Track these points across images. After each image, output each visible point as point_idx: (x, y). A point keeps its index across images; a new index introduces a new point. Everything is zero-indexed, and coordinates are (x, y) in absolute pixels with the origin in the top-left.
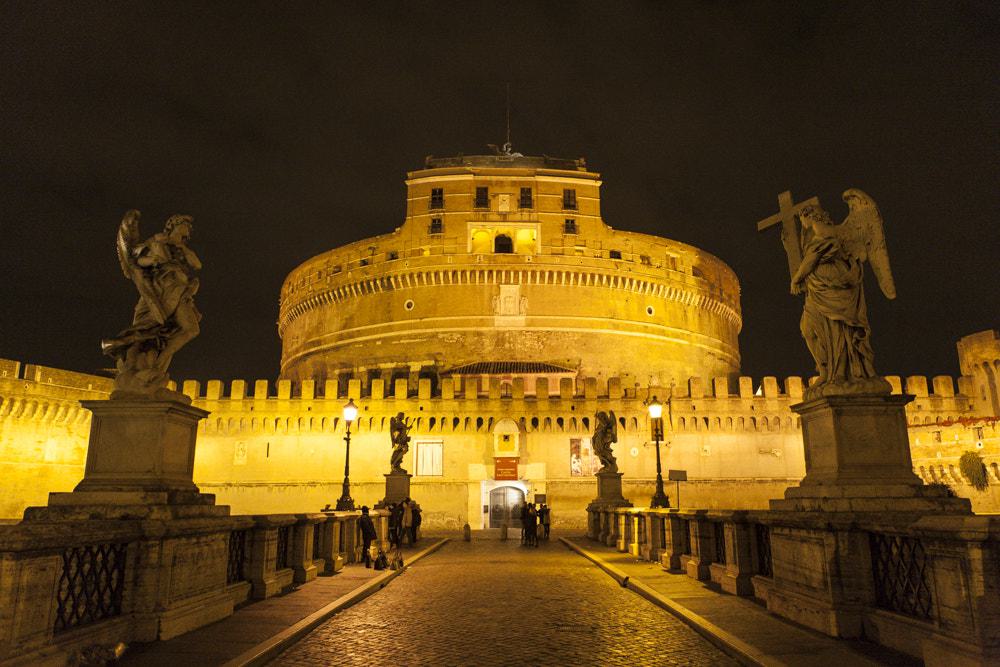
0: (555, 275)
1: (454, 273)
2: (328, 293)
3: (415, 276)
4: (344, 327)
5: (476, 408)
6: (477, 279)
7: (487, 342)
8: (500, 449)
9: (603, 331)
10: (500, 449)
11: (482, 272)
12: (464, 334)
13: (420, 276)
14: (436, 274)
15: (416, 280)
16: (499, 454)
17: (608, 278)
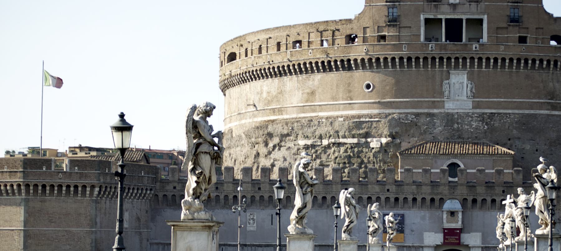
0: (500, 61)
1: (409, 59)
2: (288, 66)
3: (374, 61)
4: (307, 101)
5: (429, 191)
6: (430, 66)
7: (437, 122)
8: (447, 222)
9: (542, 112)
10: (447, 222)
11: (434, 59)
12: (417, 115)
13: (378, 59)
14: (393, 59)
15: (374, 65)
16: (447, 225)
17: (549, 62)
